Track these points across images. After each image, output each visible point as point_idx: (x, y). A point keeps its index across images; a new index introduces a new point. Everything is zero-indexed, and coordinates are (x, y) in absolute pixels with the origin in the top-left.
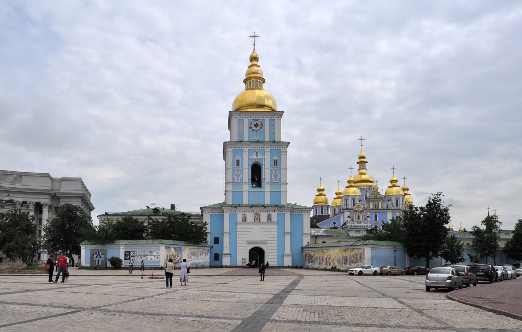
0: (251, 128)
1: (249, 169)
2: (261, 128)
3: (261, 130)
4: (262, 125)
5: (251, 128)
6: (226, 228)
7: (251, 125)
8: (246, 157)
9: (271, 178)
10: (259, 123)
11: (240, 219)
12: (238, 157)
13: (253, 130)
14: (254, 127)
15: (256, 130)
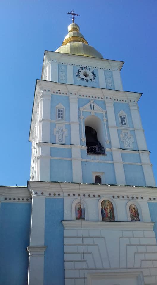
0: (79, 76)
1: (80, 125)
2: (94, 78)
3: (94, 80)
4: (95, 75)
5: (79, 76)
6: (37, 236)
7: (78, 73)
8: (74, 106)
9: (121, 142)
10: (89, 73)
11: (70, 213)
12: (60, 106)
13: (83, 79)
14: (82, 76)
15: (87, 80)
